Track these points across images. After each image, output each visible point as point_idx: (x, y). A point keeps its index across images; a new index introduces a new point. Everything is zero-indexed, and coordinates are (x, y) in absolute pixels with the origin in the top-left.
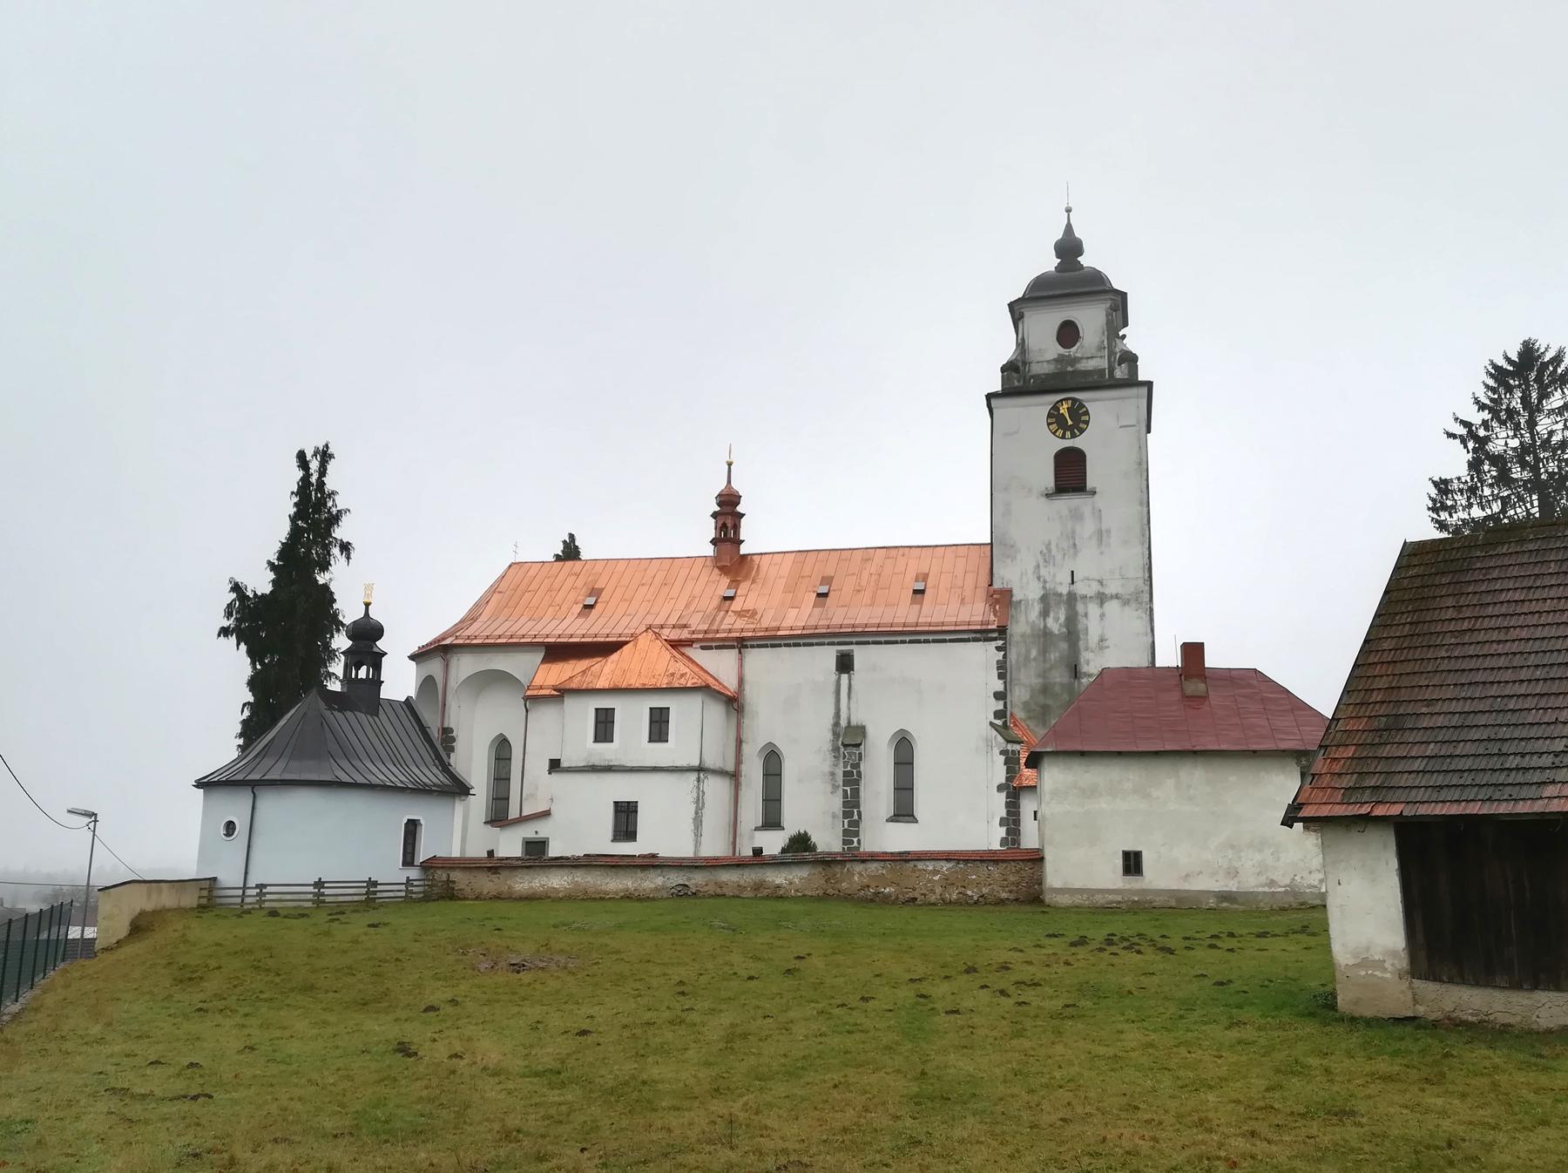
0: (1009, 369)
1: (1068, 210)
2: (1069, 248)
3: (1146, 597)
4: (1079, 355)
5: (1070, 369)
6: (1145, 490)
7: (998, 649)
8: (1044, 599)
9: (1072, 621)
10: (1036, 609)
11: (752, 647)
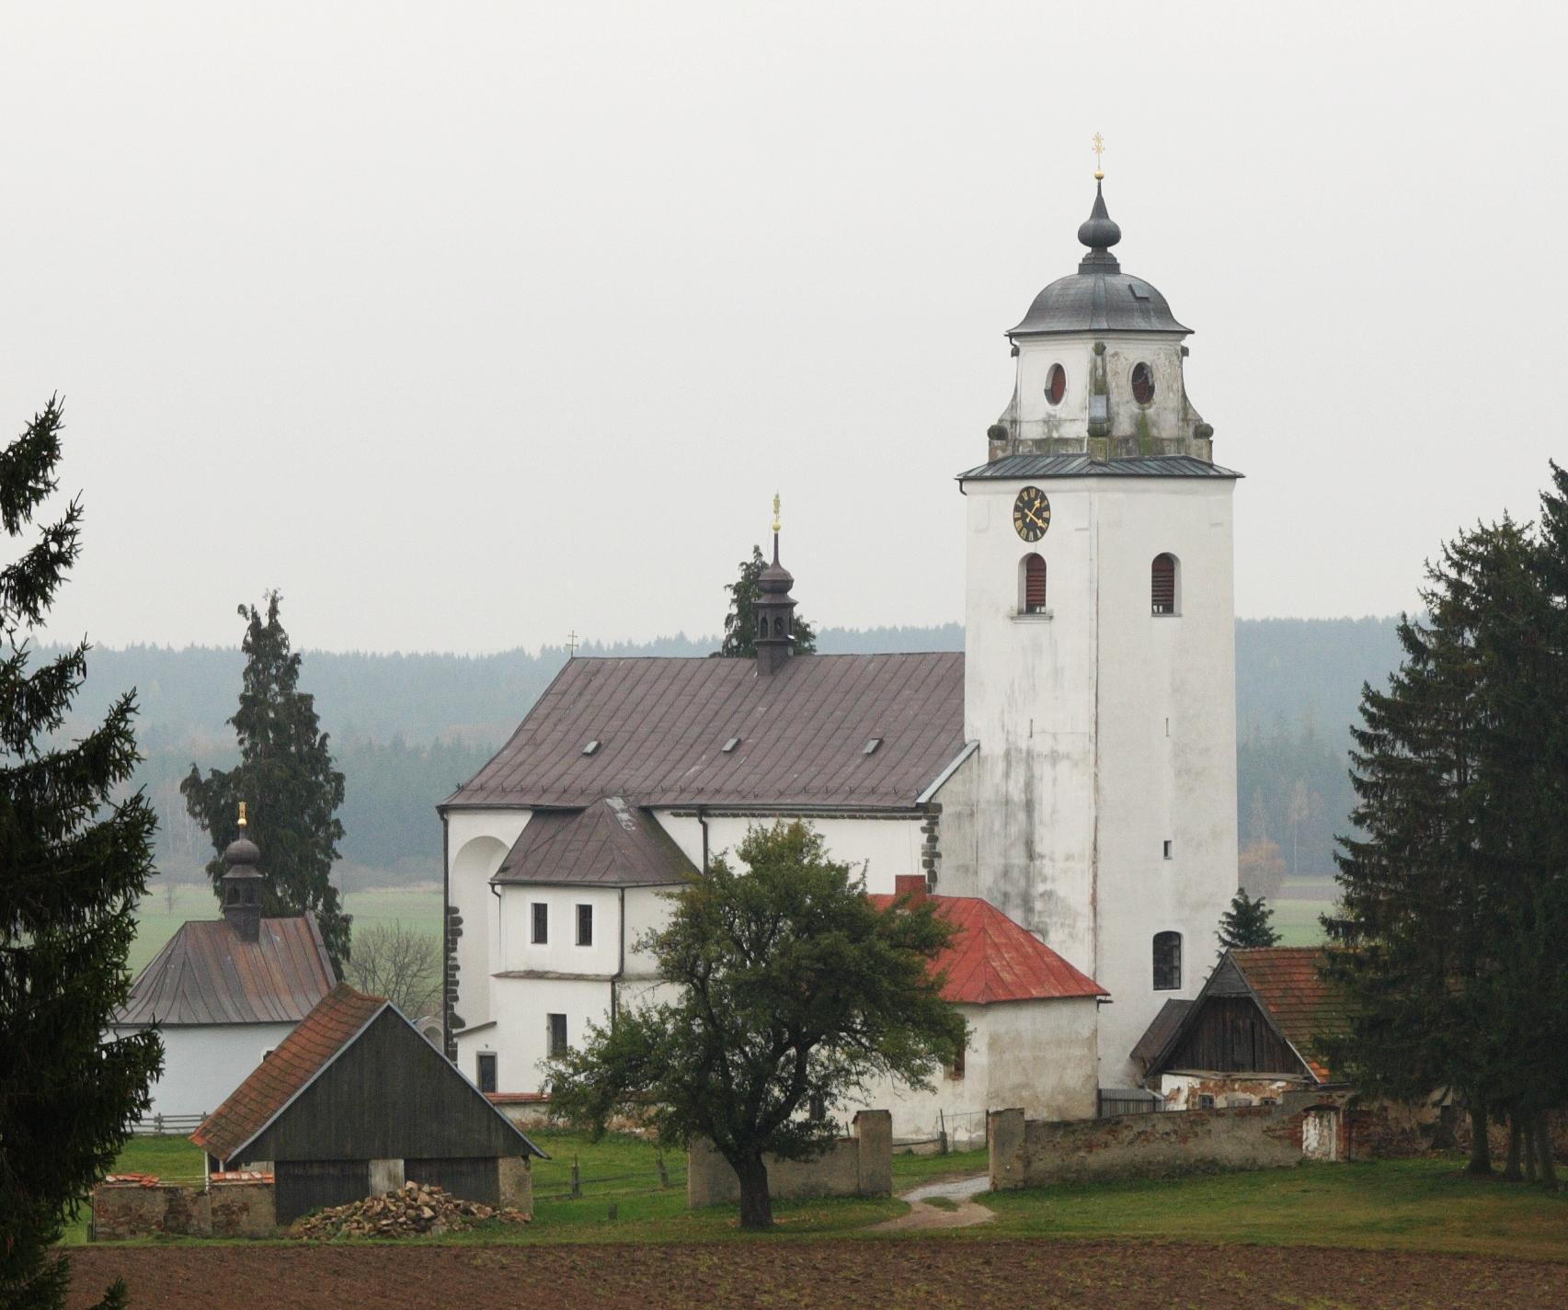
0: (997, 433)
1: (1100, 178)
2: (1100, 237)
3: (1092, 757)
4: (1063, 416)
5: (1055, 435)
6: (1094, 616)
7: (924, 830)
8: (1007, 754)
9: (1029, 786)
10: (1001, 766)
11: (716, 816)
